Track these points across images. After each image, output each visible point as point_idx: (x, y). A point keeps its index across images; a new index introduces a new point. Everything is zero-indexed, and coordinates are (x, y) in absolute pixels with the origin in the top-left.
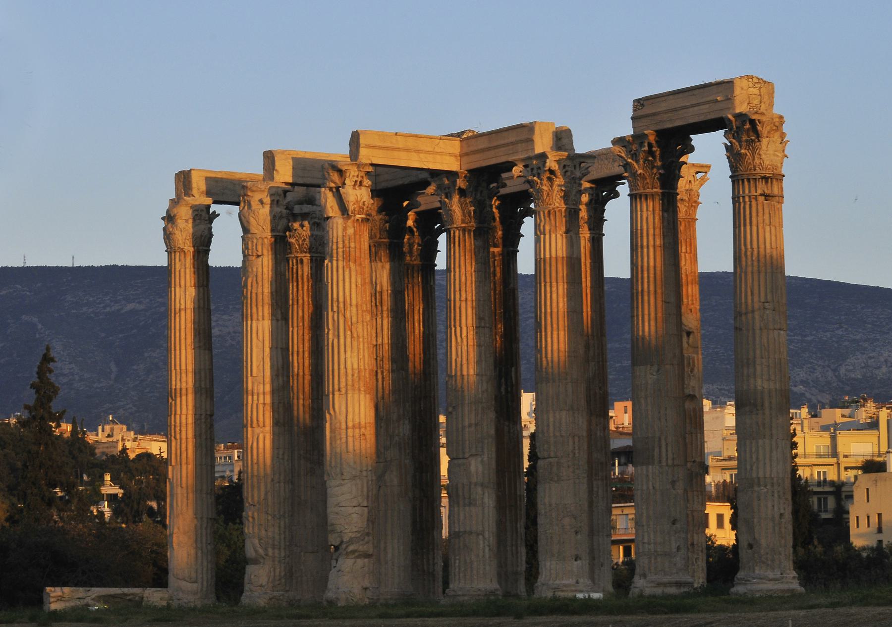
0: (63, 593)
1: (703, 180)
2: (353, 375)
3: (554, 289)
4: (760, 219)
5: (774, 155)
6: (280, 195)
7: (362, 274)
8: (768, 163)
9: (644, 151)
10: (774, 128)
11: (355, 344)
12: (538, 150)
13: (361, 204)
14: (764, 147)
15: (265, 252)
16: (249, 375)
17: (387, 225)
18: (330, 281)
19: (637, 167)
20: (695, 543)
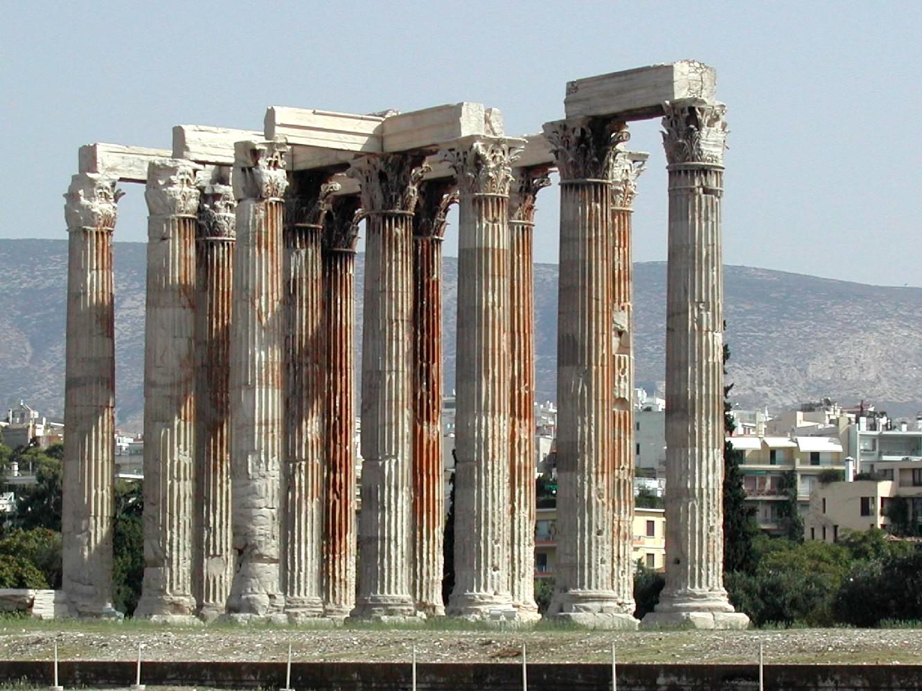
6: (190, 175)
9: (577, 138)
12: (465, 132)
20: (621, 555)
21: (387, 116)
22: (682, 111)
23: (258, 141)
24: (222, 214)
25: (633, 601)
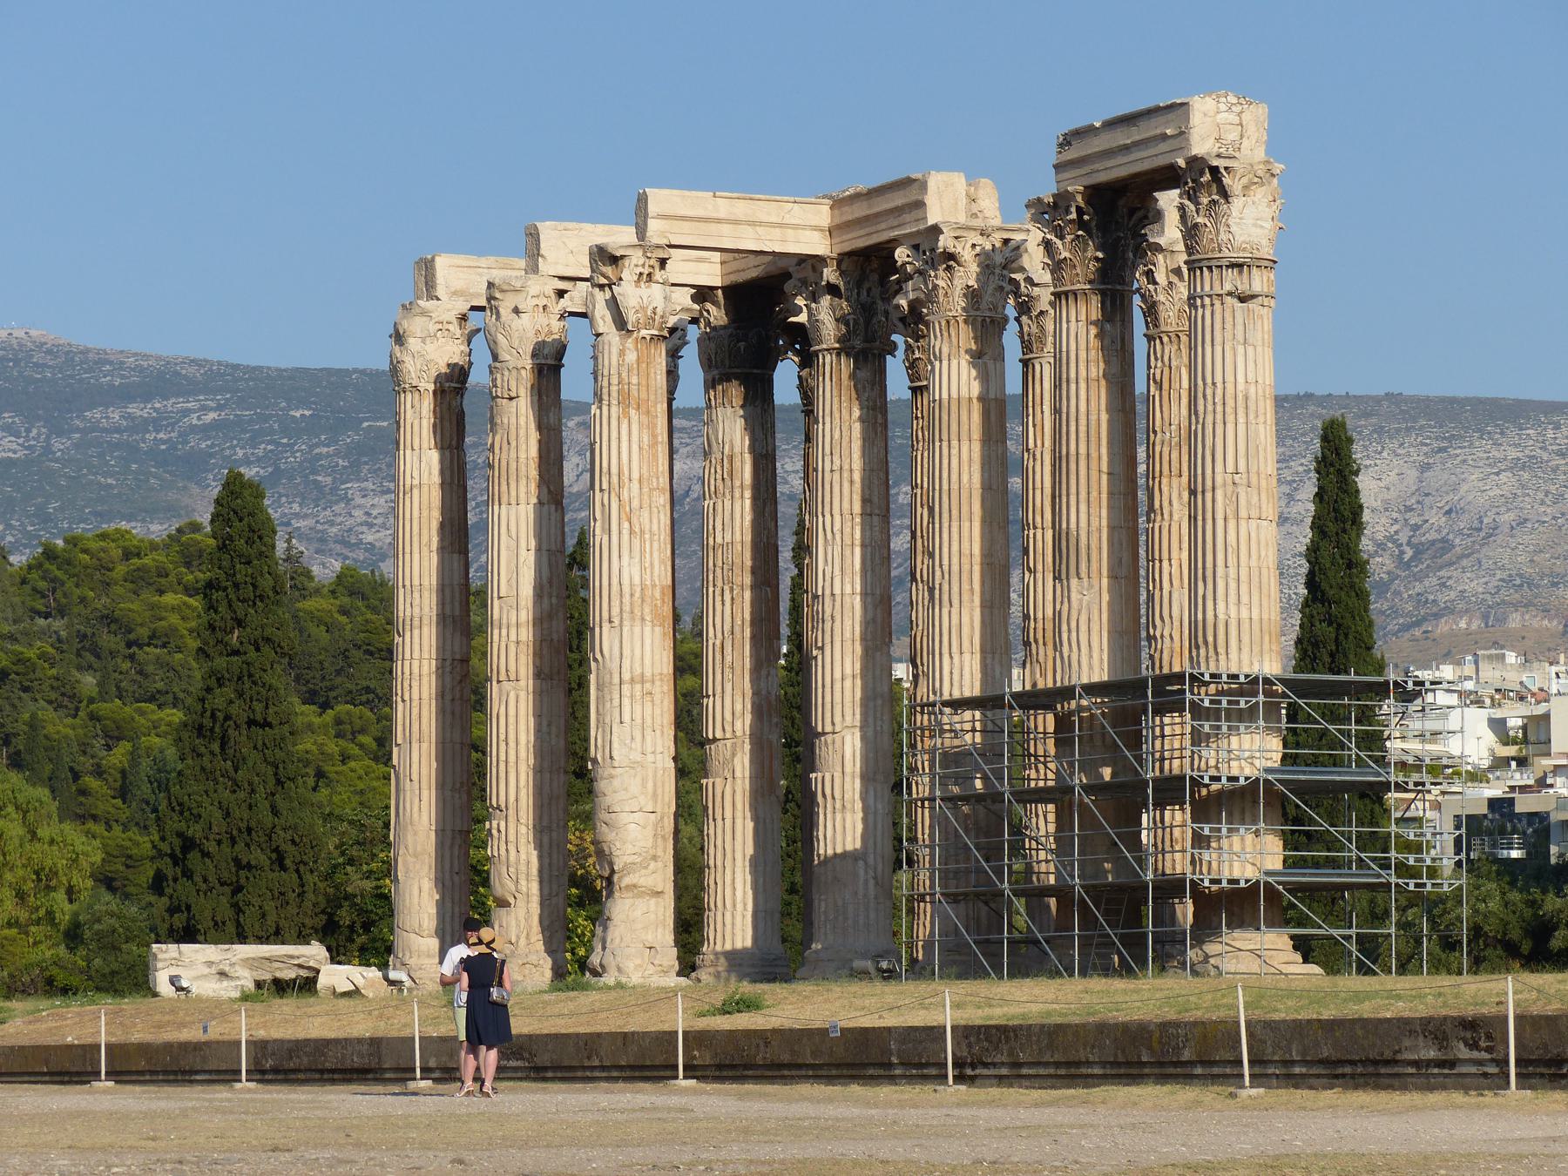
0: (180, 953)
2: (632, 595)
3: (954, 451)
4: (1228, 335)
5: (1255, 225)
7: (652, 427)
8: (1242, 239)
9: (1071, 221)
10: (1256, 180)
11: (636, 542)
12: (931, 222)
13: (649, 313)
15: (522, 392)
16: (495, 595)
17: (742, 345)
18: (598, 440)
19: (1061, 247)
22: (1202, 174)
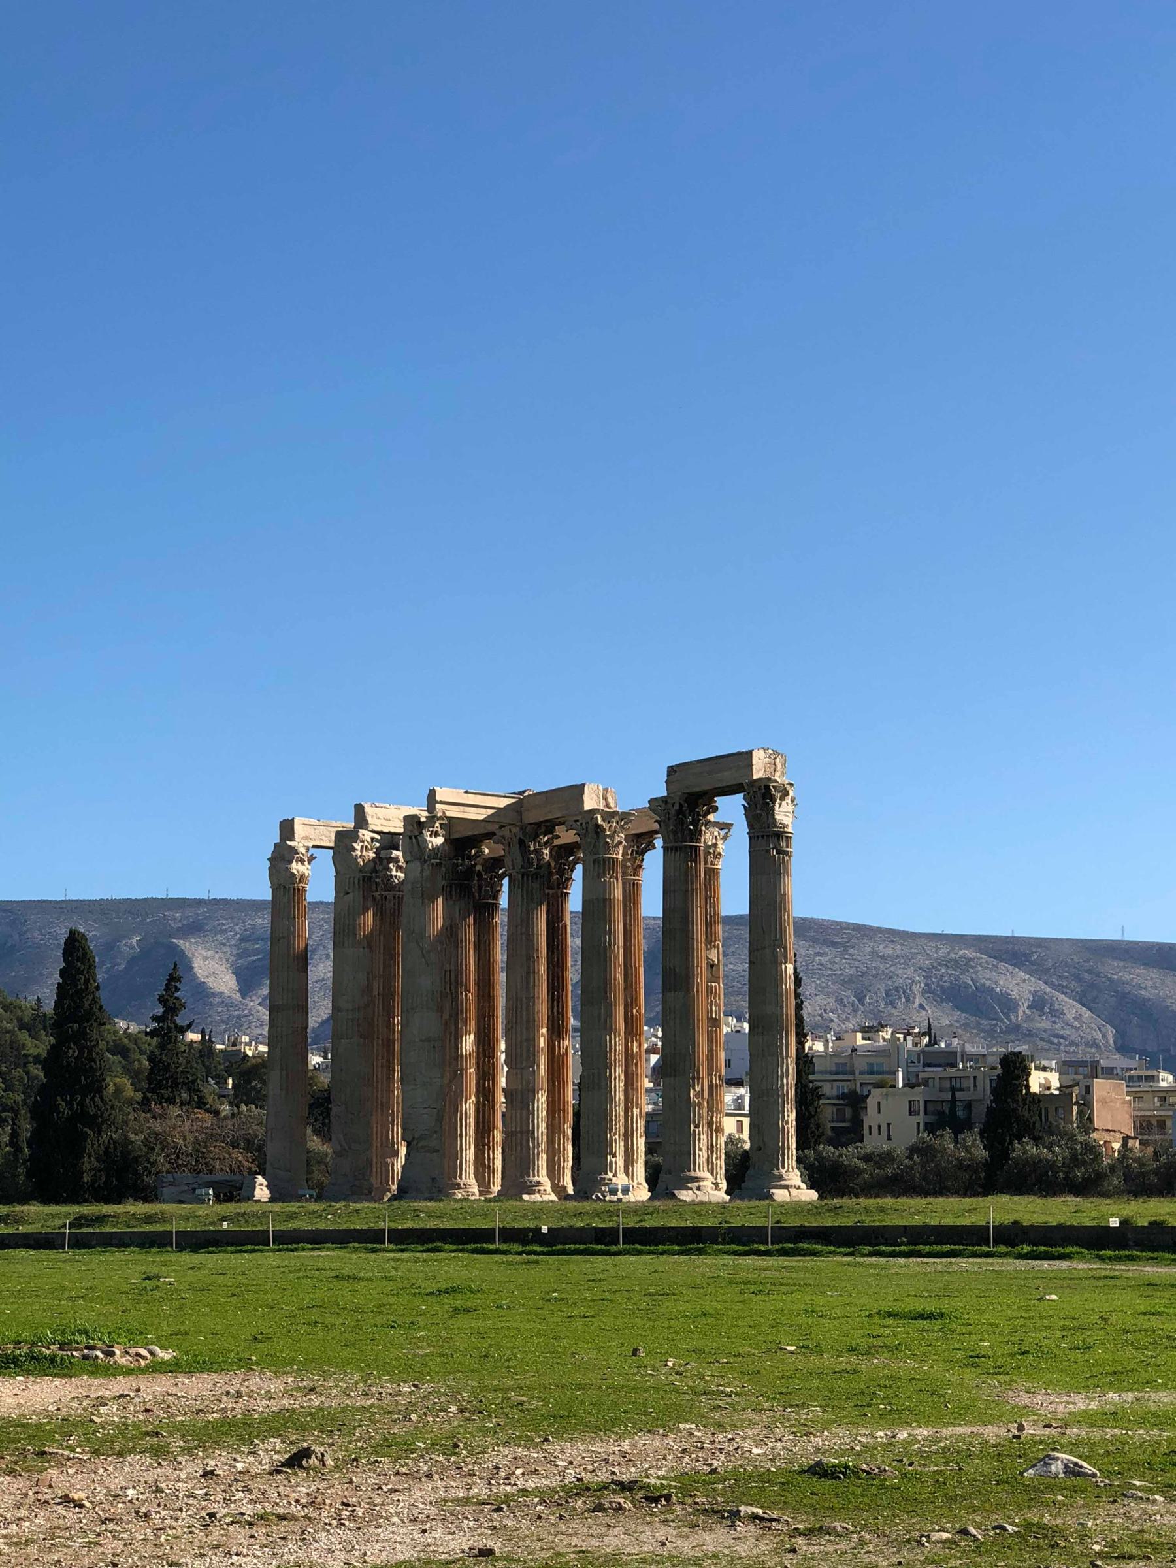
1: (725, 838)
12: (587, 807)
14: (777, 808)
21: (526, 794)
23: (424, 816)
24: (394, 873)
25: (724, 1182)
